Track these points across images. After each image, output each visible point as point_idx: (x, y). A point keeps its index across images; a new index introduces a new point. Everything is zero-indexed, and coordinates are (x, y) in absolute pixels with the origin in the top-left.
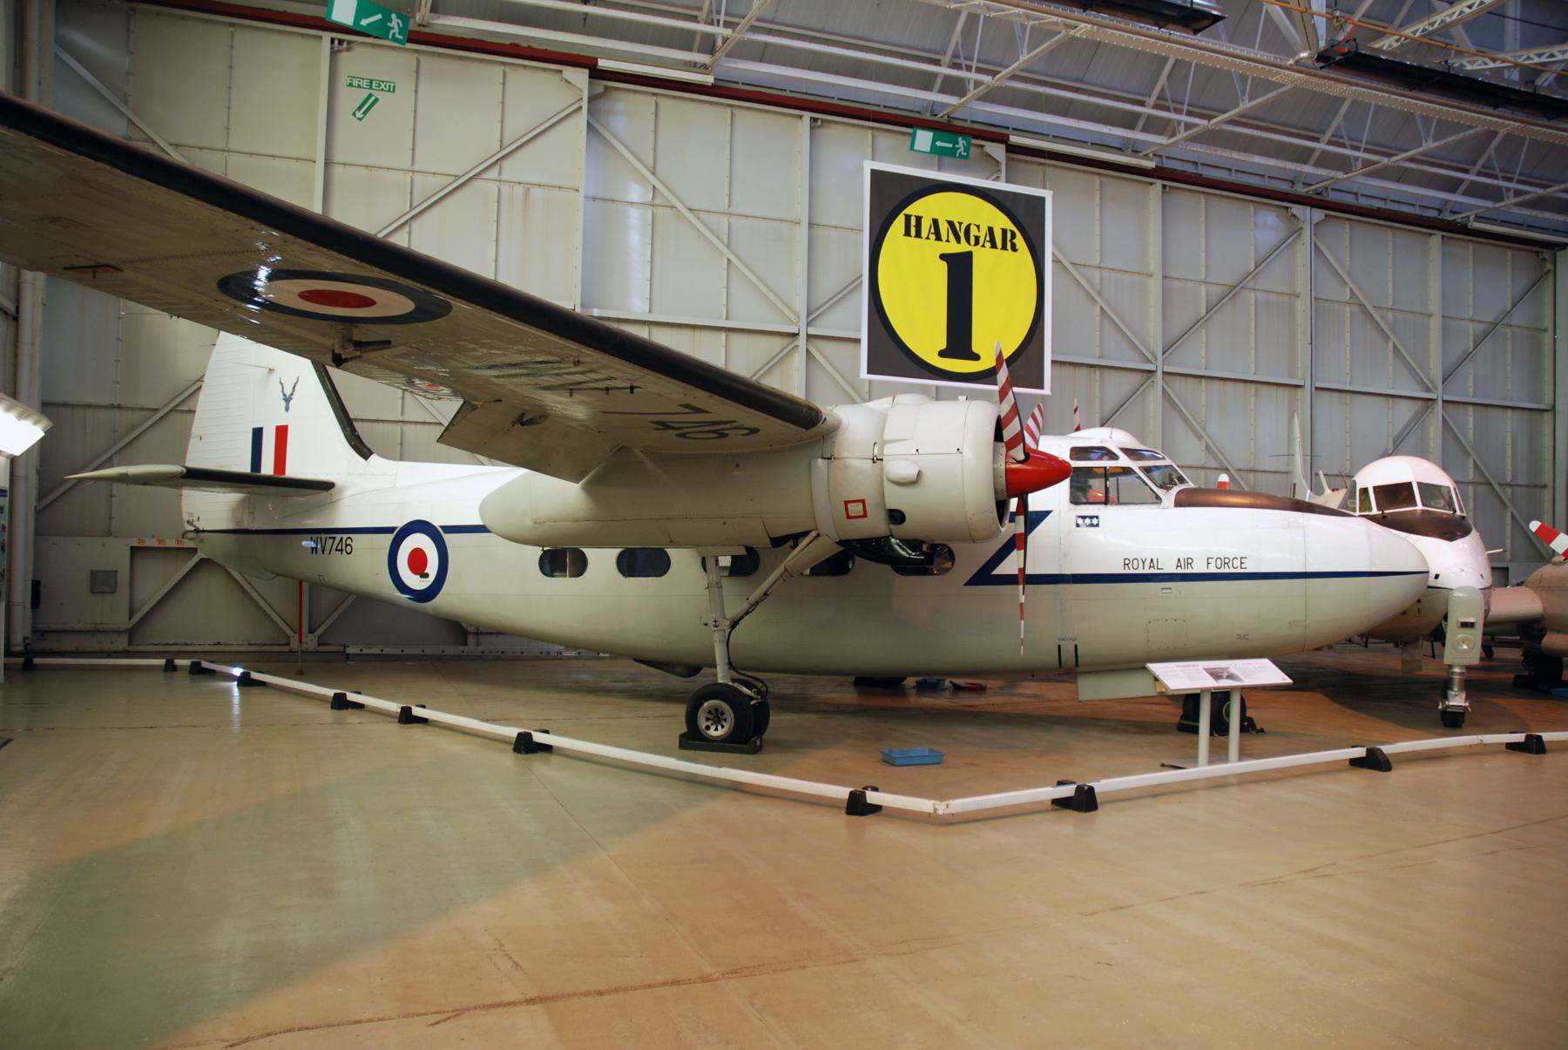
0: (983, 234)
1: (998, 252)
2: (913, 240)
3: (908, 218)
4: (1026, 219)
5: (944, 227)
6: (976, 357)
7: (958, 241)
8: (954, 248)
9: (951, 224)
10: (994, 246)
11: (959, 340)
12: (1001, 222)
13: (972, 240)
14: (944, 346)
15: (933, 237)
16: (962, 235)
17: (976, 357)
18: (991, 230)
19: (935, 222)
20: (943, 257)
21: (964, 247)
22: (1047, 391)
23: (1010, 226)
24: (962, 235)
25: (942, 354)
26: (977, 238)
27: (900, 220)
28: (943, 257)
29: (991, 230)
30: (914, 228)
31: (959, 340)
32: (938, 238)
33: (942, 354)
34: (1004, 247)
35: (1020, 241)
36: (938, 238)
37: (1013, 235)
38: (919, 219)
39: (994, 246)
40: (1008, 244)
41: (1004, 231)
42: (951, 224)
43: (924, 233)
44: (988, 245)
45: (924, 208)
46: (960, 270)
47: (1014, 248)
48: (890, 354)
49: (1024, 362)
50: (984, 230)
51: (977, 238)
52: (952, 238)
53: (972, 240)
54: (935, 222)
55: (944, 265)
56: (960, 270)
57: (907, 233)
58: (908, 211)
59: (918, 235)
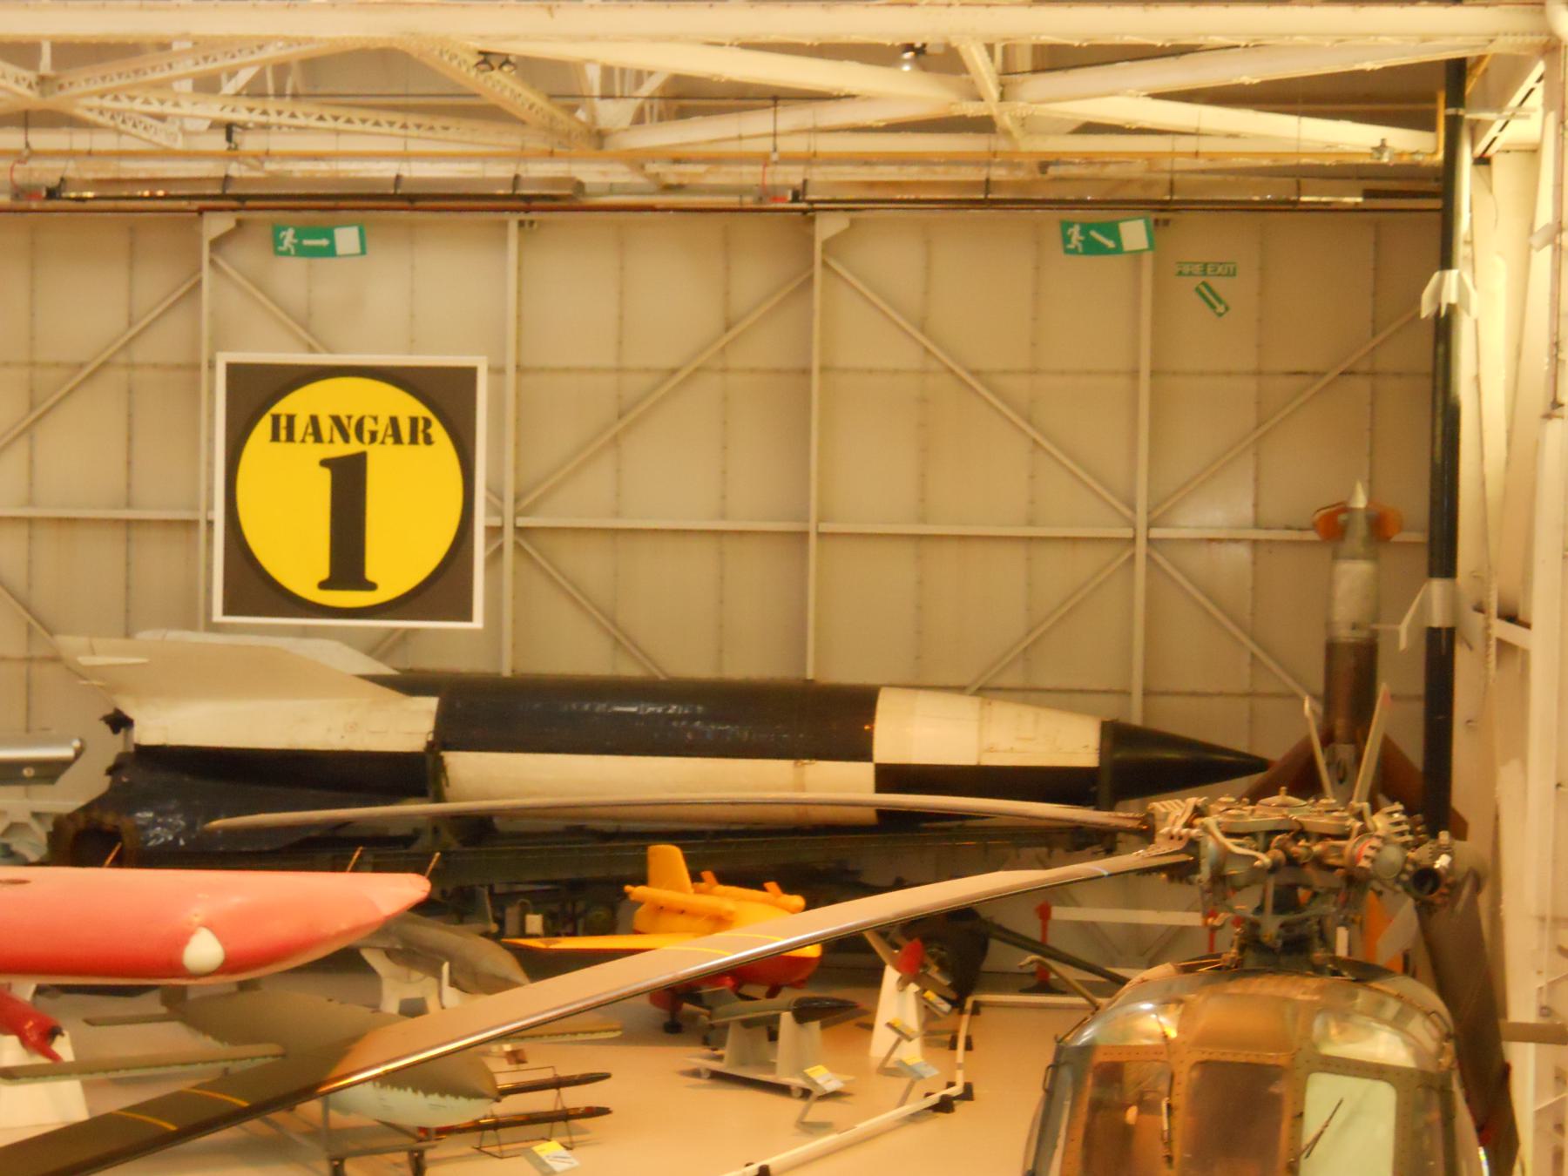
0: (382, 427)
1: (406, 449)
2: (282, 447)
3: (276, 419)
4: (445, 397)
5: (326, 425)
6: (371, 587)
7: (346, 439)
8: (340, 449)
9: (336, 420)
10: (398, 439)
11: (347, 563)
12: (407, 407)
13: (367, 437)
14: (324, 573)
15: (310, 439)
16: (352, 432)
17: (371, 587)
18: (394, 422)
19: (314, 420)
20: (325, 463)
21: (354, 447)
22: (478, 622)
23: (421, 411)
24: (352, 432)
25: (323, 585)
26: (373, 435)
27: (265, 425)
28: (325, 463)
29: (394, 422)
30: (284, 431)
31: (347, 563)
32: (318, 438)
33: (323, 585)
34: (414, 440)
35: (438, 431)
36: (318, 438)
37: (428, 423)
38: (291, 419)
39: (398, 439)
40: (418, 434)
41: (414, 421)
42: (336, 420)
43: (299, 432)
44: (390, 440)
45: (299, 404)
46: (348, 481)
47: (428, 440)
48: (253, 589)
49: (444, 590)
50: (384, 422)
51: (373, 435)
52: (337, 436)
53: (367, 437)
54: (314, 420)
55: (326, 474)
56: (348, 481)
57: (275, 437)
58: (276, 409)
59: (290, 438)
